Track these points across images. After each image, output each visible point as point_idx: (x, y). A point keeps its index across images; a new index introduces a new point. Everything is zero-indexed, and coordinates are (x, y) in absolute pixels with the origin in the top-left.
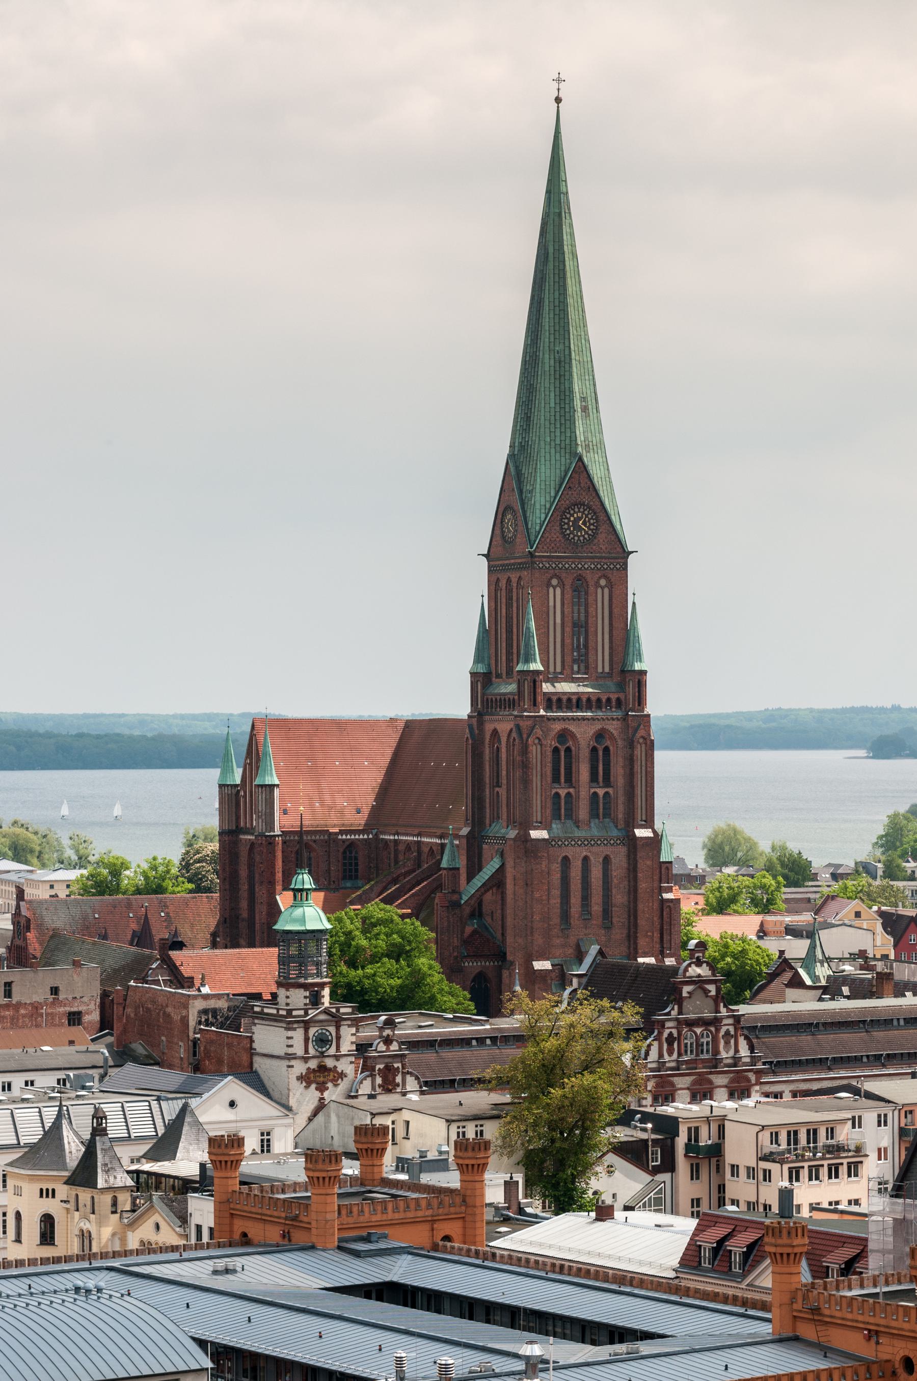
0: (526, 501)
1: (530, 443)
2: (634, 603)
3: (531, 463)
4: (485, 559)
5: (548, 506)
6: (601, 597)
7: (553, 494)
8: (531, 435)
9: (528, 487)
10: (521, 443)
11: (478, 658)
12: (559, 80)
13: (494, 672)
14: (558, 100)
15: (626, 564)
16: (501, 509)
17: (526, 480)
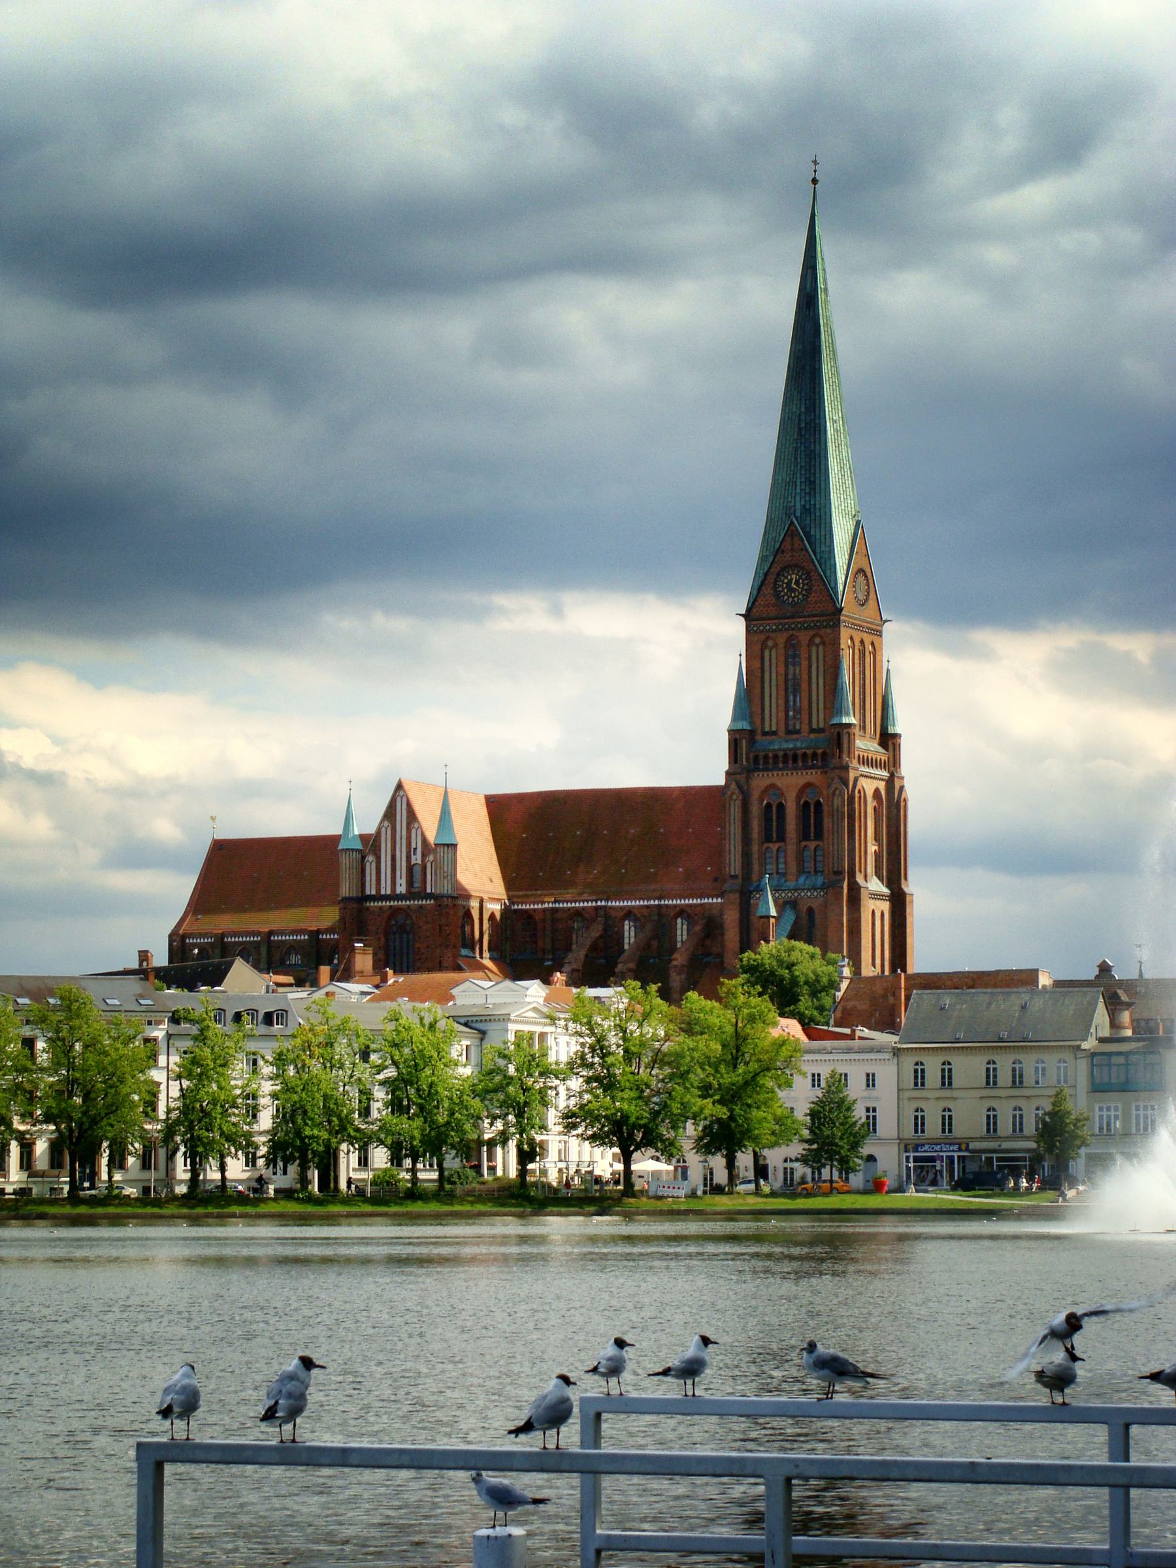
0: (823, 561)
1: (818, 506)
2: (888, 671)
3: (823, 525)
4: (742, 619)
5: (845, 567)
6: (869, 659)
7: (847, 557)
8: (818, 499)
9: (823, 549)
10: (804, 506)
11: (735, 718)
12: (815, 162)
13: (759, 732)
14: (815, 181)
15: (881, 632)
16: (775, 570)
17: (818, 541)
